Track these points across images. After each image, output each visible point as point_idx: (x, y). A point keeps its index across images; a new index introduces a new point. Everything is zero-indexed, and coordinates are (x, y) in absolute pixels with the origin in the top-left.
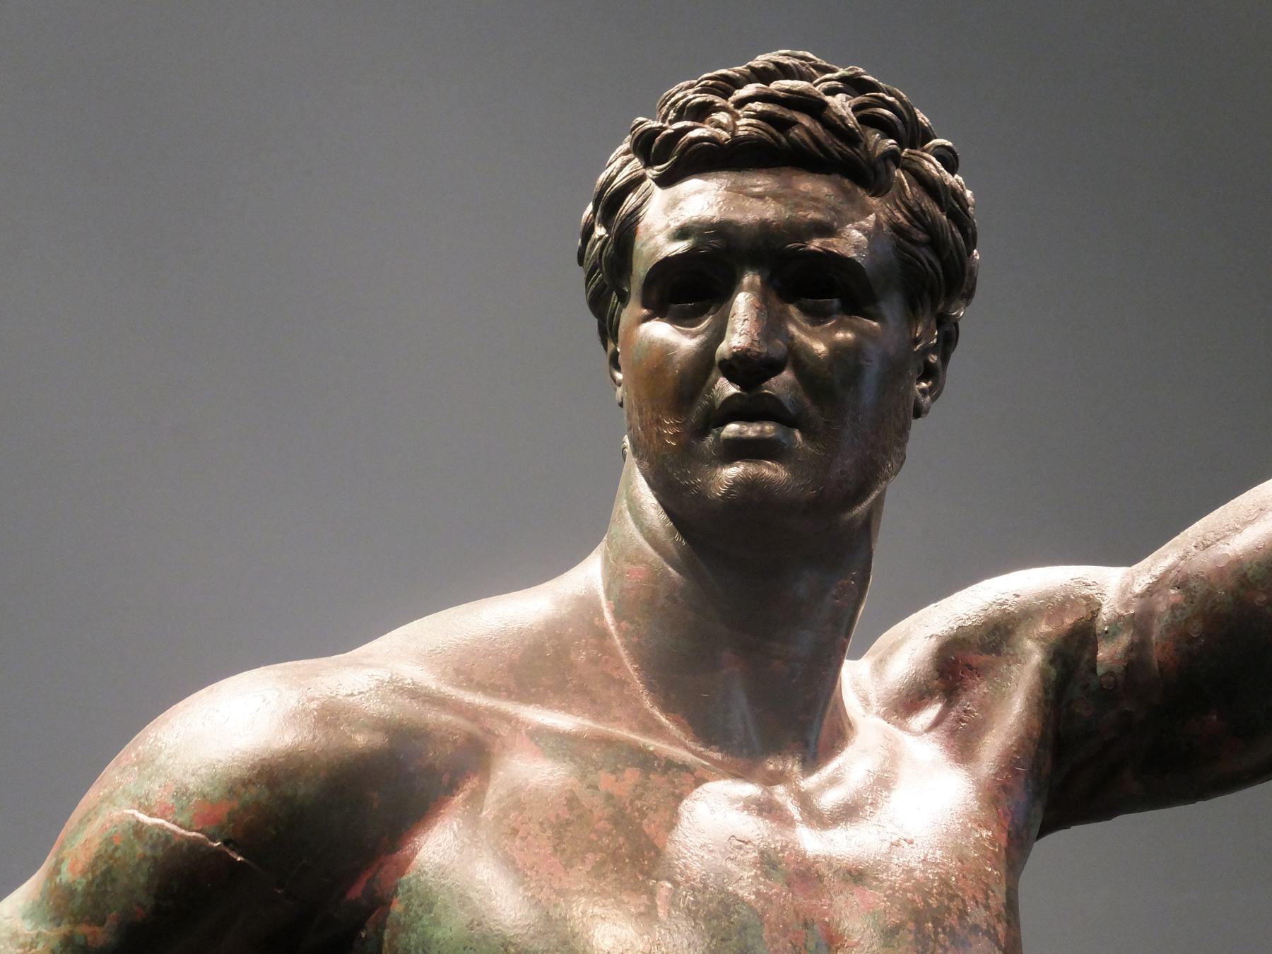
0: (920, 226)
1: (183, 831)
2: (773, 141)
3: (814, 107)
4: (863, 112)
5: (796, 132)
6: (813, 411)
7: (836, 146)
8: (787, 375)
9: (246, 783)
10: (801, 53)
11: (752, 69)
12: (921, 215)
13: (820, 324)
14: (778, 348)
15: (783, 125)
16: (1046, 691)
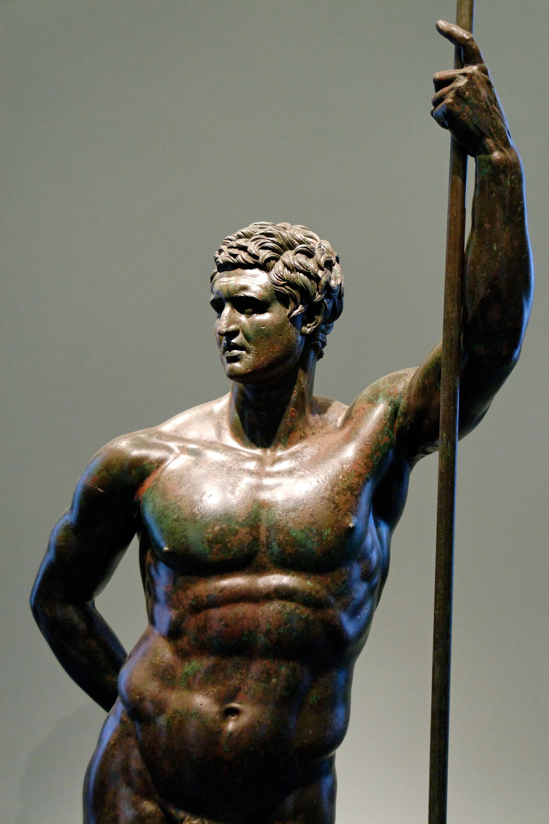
0: (281, 279)
1: (88, 484)
2: (233, 262)
3: (244, 249)
4: (262, 246)
5: (239, 258)
6: (248, 345)
7: (250, 260)
8: (241, 336)
9: (102, 470)
10: (259, 223)
11: (243, 233)
12: (282, 277)
13: (249, 317)
14: (232, 327)
15: (235, 256)
16: (385, 415)
